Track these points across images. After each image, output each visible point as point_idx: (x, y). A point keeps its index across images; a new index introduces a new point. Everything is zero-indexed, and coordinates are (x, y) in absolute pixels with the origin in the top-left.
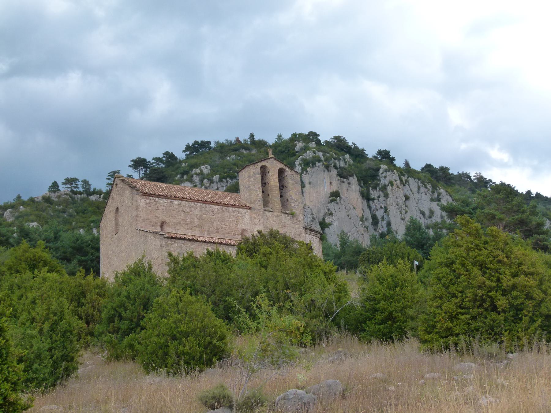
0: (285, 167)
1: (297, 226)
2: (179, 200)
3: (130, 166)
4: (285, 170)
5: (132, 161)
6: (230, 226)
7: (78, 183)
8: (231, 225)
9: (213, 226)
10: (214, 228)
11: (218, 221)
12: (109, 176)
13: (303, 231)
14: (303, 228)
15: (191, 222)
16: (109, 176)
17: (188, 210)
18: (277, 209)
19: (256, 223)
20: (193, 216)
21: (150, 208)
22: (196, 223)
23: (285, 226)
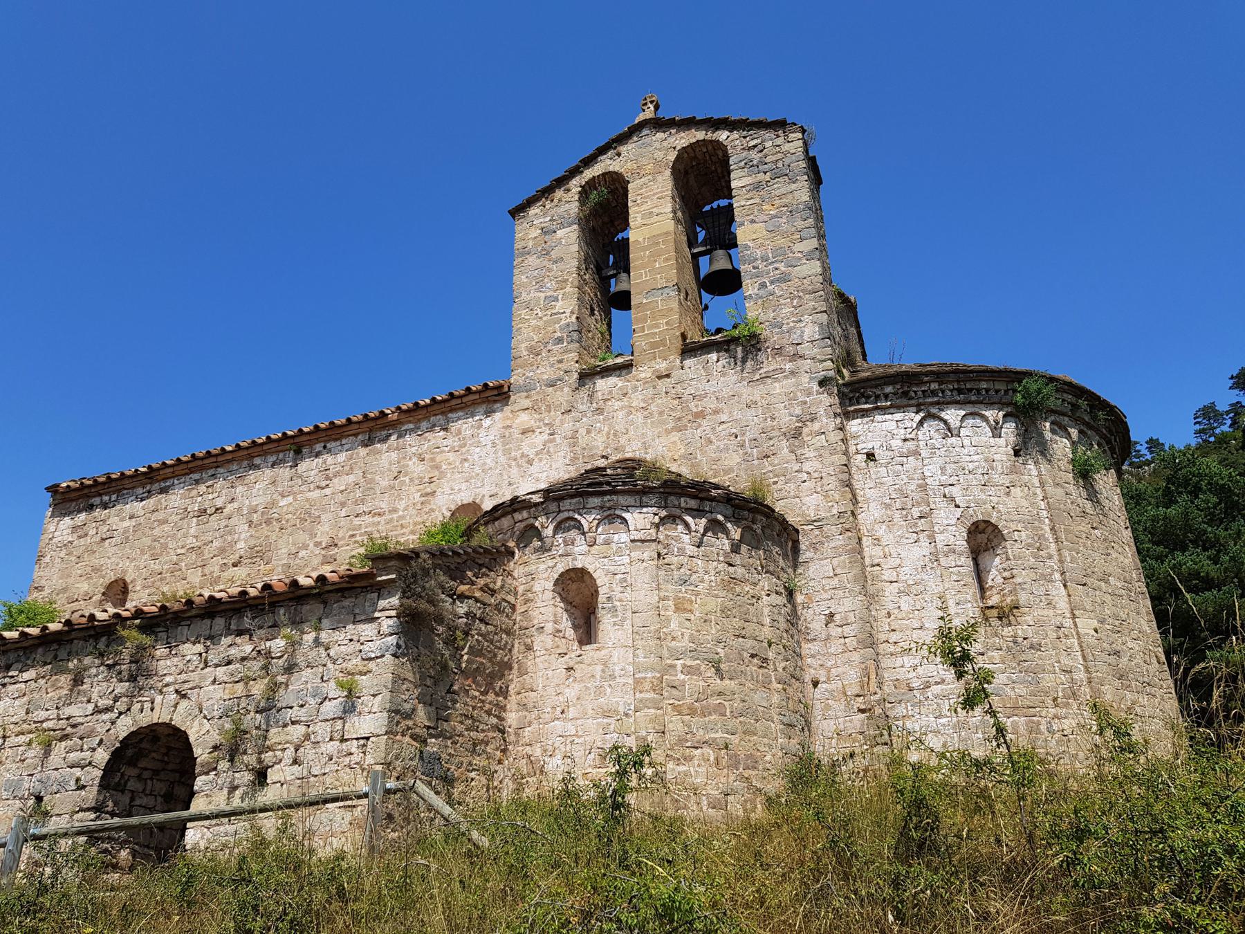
0: (710, 136)
1: (778, 388)
2: (191, 471)
3: (1230, 388)
4: (717, 145)
5: (1232, 378)
6: (395, 510)
7: (1138, 447)
8: (401, 505)
9: (313, 535)
10: (317, 544)
11: (343, 504)
12: (1195, 418)
13: (825, 402)
14: (822, 383)
15: (222, 551)
16: (1195, 418)
17: (219, 503)
18: (654, 346)
19: (531, 453)
20: (234, 521)
21: (82, 541)
22: (241, 545)
23: (701, 415)
